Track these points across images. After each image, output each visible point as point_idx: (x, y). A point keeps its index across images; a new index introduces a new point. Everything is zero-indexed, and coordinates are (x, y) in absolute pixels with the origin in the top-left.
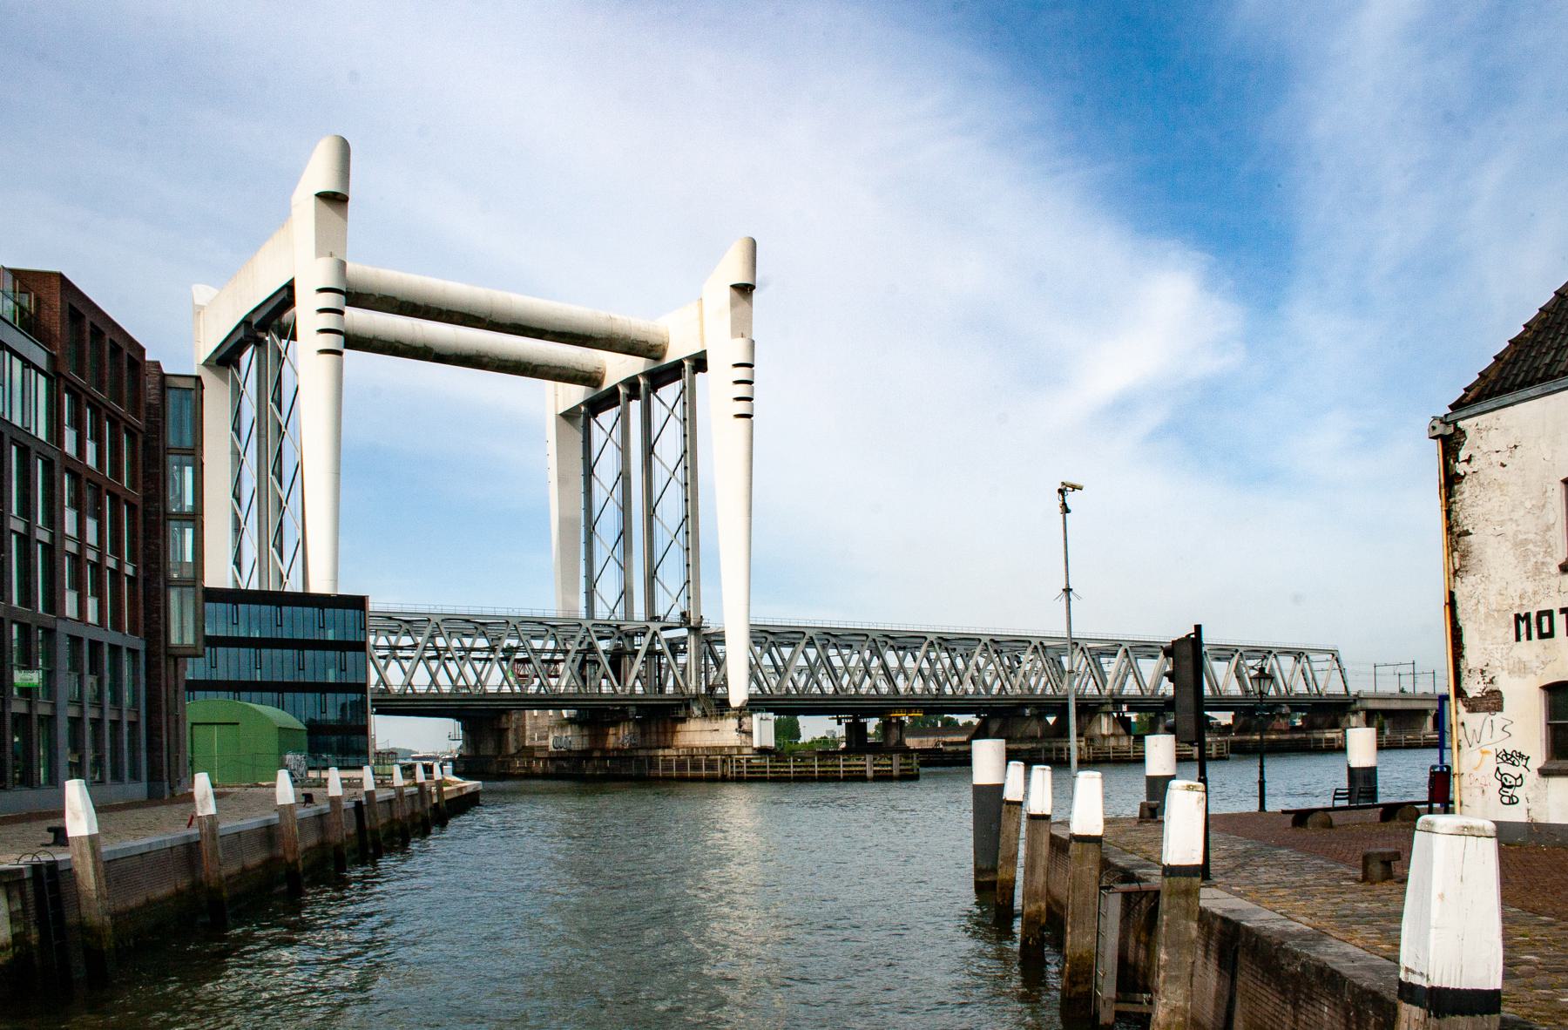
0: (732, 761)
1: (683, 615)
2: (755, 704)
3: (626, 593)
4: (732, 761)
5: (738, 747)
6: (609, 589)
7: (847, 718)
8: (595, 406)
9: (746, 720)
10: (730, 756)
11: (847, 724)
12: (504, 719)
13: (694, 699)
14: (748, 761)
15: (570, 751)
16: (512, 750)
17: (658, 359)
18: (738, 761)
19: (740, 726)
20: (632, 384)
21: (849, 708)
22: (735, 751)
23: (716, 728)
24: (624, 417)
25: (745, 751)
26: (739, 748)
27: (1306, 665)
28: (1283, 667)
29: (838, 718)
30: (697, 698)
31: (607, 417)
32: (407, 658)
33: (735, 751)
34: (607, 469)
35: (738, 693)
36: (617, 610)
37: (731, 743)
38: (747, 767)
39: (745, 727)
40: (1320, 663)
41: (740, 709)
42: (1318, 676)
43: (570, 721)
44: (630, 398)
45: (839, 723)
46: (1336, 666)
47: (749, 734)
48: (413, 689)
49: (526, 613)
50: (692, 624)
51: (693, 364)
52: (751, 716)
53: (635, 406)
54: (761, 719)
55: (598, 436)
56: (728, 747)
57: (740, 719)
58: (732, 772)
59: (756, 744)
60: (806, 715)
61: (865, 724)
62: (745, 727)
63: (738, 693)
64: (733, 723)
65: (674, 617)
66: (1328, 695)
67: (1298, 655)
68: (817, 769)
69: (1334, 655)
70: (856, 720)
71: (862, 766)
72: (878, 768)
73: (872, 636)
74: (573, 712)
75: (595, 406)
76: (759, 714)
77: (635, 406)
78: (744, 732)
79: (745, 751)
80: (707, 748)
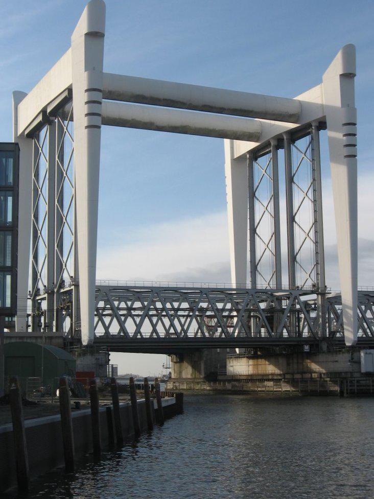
0: (347, 382)
4: (347, 382)
5: (351, 372)
8: (255, 155)
9: (355, 354)
10: (346, 378)
14: (358, 381)
18: (351, 382)
19: (352, 359)
22: (349, 375)
23: (336, 360)
25: (356, 375)
30: (324, 338)
36: (271, 283)
38: (358, 386)
39: (356, 359)
41: (352, 347)
47: (359, 362)
48: (141, 335)
49: (213, 286)
52: (360, 352)
53: (281, 153)
54: (366, 353)
59: (363, 370)
62: (356, 359)
65: (308, 286)
76: (365, 351)
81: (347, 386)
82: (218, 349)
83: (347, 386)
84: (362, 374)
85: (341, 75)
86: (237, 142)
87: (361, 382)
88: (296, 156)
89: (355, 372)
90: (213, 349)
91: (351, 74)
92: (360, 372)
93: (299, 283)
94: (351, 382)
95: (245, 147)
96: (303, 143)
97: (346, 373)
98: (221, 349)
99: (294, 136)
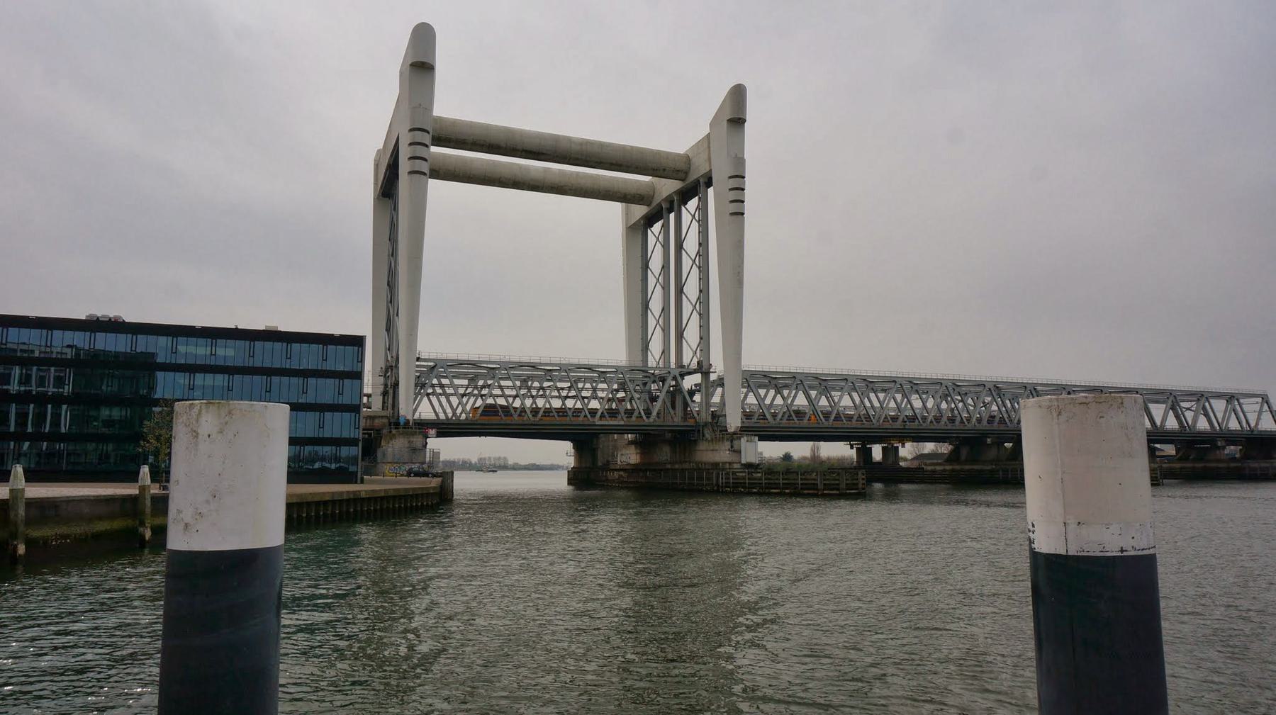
1: (698, 363)
2: (745, 430)
3: (665, 352)
6: (656, 347)
7: (858, 444)
9: (736, 442)
10: (723, 470)
11: (857, 448)
12: (595, 441)
13: (703, 426)
15: (629, 464)
16: (600, 464)
17: (683, 180)
18: (728, 474)
19: (732, 447)
20: (670, 200)
21: (861, 436)
24: (665, 227)
26: (730, 463)
27: (1238, 407)
28: (1215, 410)
29: (850, 444)
30: (706, 424)
31: (657, 227)
32: (510, 396)
33: (727, 466)
34: (656, 264)
35: (733, 421)
37: (726, 460)
39: (736, 447)
40: (1251, 406)
41: (734, 433)
42: (1249, 416)
43: (631, 443)
44: (670, 211)
45: (852, 448)
46: (1266, 407)
50: (704, 370)
51: (707, 181)
52: (740, 439)
55: (651, 240)
56: (722, 463)
57: (732, 442)
58: (722, 483)
60: (780, 441)
61: (871, 448)
62: (736, 447)
63: (733, 421)
64: (727, 444)
65: (694, 365)
66: (1258, 431)
67: (1230, 398)
68: (800, 482)
69: (1265, 399)
70: (864, 445)
71: (814, 480)
72: (827, 482)
73: (850, 379)
74: (634, 436)
75: (649, 221)
77: (672, 216)
78: (734, 451)
79: (736, 466)
80: (708, 463)
81: (722, 478)
82: (616, 435)
83: (722, 478)
84: (742, 465)
85: (728, 120)
86: (633, 206)
87: (737, 474)
88: (686, 217)
89: (733, 463)
90: (611, 435)
91: (740, 119)
92: (740, 462)
93: (686, 361)
94: (728, 474)
95: (640, 211)
96: (693, 204)
97: (724, 463)
98: (619, 435)
99: (685, 195)
